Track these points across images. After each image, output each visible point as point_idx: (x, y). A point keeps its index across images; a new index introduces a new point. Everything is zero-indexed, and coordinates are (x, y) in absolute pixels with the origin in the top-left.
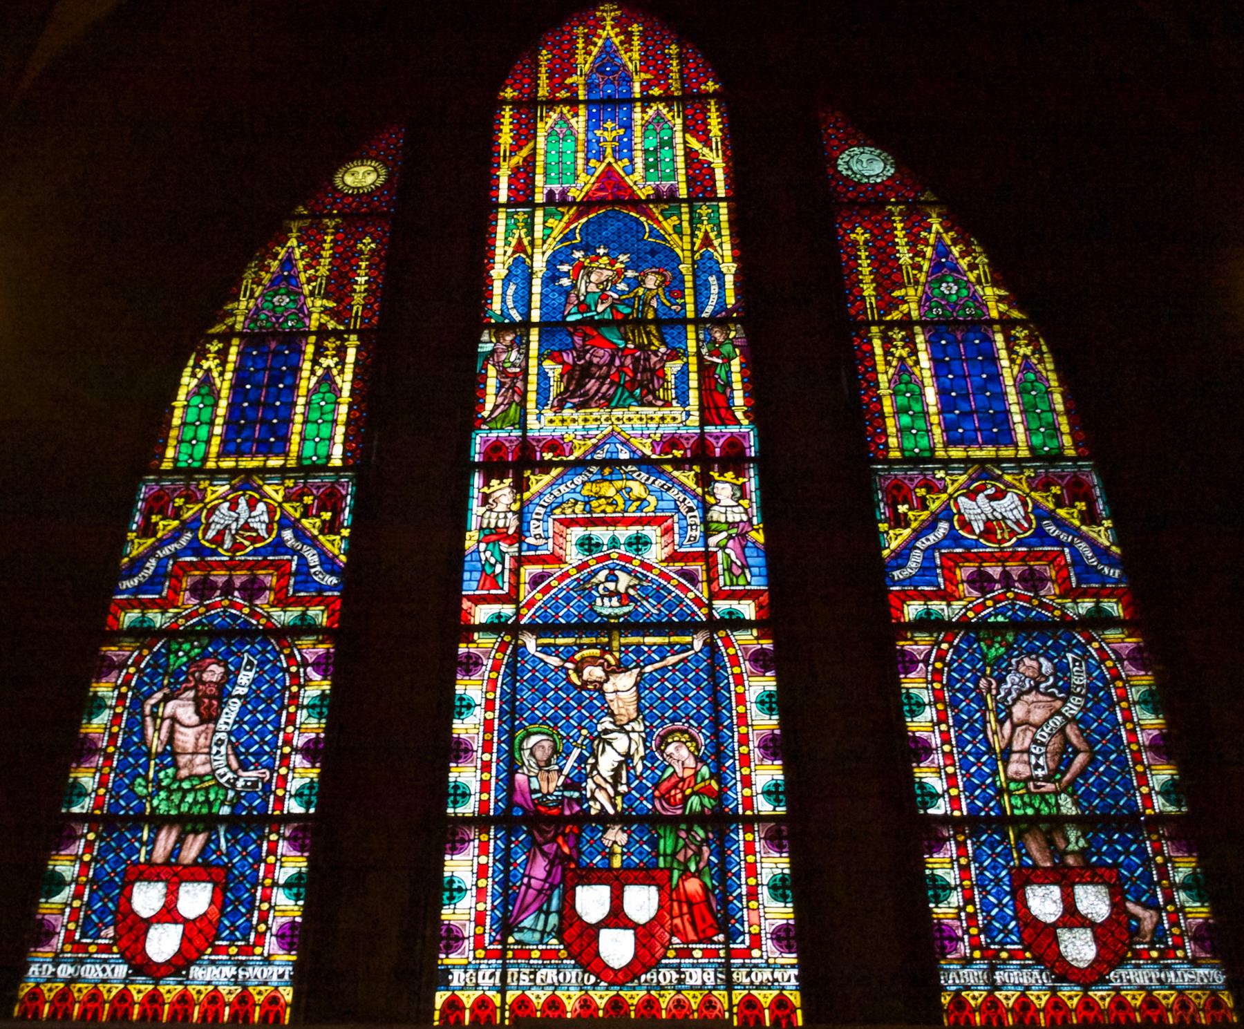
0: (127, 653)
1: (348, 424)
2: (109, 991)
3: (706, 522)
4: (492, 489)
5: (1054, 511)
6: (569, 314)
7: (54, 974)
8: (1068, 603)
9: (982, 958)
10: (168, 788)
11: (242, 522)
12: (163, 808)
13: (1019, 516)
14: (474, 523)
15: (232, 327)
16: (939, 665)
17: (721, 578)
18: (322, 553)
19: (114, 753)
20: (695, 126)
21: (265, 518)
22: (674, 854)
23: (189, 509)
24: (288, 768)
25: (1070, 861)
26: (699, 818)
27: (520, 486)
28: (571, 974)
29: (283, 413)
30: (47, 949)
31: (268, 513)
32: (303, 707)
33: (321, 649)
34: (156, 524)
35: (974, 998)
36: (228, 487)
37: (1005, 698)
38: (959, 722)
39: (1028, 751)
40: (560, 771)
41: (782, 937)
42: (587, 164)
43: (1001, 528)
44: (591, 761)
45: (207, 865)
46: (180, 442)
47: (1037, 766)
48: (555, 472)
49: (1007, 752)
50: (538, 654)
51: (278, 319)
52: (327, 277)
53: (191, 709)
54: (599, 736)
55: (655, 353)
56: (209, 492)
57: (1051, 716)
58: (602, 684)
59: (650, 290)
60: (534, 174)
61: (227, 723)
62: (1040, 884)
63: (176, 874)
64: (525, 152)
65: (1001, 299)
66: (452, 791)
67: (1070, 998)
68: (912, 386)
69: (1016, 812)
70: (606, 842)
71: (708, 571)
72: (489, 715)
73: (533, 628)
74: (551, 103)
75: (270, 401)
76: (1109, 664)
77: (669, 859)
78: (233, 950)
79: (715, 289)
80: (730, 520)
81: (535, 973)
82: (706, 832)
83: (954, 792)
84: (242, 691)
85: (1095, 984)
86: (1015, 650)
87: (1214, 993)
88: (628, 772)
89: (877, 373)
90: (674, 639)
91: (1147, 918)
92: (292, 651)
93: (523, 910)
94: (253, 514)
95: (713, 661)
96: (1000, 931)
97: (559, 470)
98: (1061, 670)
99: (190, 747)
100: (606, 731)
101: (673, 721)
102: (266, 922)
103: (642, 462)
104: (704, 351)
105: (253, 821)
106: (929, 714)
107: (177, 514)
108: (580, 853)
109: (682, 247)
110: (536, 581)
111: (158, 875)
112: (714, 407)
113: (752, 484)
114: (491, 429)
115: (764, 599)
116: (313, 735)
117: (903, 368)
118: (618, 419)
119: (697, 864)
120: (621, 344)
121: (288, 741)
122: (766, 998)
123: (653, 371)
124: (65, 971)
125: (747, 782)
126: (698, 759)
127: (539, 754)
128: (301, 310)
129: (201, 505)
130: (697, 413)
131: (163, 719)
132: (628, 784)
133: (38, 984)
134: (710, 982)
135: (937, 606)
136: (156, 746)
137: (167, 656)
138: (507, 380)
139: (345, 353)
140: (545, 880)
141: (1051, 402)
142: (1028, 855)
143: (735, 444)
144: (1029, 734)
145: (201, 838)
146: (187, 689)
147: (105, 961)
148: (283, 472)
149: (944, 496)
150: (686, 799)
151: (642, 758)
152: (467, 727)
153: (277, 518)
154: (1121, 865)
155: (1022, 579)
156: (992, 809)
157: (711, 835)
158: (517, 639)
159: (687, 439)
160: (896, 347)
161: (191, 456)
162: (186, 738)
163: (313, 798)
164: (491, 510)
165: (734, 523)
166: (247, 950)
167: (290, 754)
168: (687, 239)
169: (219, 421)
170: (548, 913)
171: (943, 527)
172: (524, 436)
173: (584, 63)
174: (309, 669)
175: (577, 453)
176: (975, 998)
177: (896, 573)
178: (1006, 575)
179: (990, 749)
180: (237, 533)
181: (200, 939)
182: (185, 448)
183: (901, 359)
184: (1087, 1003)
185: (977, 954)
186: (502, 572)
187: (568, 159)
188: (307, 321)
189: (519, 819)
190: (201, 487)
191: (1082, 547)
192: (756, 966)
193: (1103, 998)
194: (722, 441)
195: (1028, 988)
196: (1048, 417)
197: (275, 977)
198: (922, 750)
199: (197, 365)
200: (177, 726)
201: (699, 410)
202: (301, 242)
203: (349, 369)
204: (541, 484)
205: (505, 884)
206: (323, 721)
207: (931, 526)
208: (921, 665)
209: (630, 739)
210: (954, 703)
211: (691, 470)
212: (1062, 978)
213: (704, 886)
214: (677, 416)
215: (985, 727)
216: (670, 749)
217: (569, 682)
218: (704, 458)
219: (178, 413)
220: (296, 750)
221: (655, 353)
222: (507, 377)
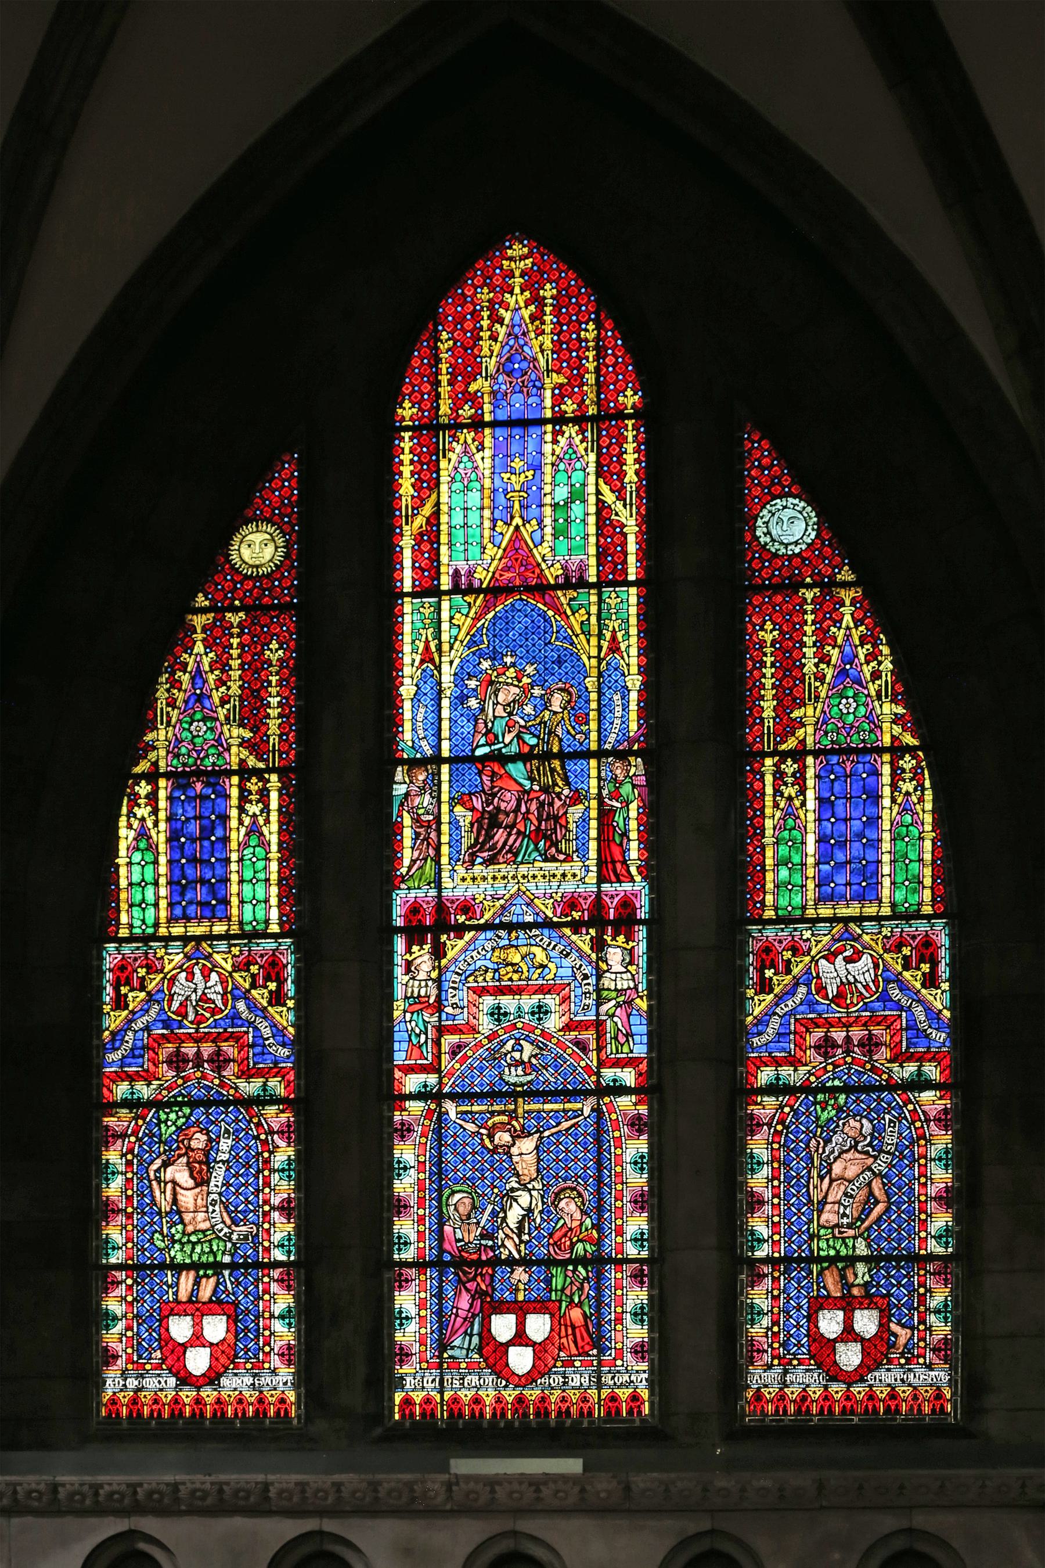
0: (126, 1124)
1: (279, 884)
2: (166, 1396)
3: (598, 990)
4: (414, 956)
5: (900, 974)
6: (478, 746)
7: (125, 1385)
8: (895, 1067)
9: (779, 1365)
10: (180, 1241)
11: (200, 993)
12: (179, 1258)
13: (869, 979)
14: (399, 992)
15: (155, 765)
16: (779, 1128)
17: (609, 1046)
18: (274, 1025)
19: (133, 1213)
20: (608, 469)
21: (219, 988)
22: (563, 1290)
23: (152, 980)
24: (269, 1223)
25: (855, 1291)
26: (583, 1261)
27: (438, 952)
28: (490, 1379)
29: (219, 871)
30: (115, 1368)
31: (222, 983)
32: (275, 1171)
33: (284, 1117)
34: (126, 996)
35: (769, 1393)
36: (181, 955)
37: (829, 1156)
38: (788, 1178)
39: (839, 1203)
40: (478, 1223)
41: (639, 1351)
42: (493, 529)
43: (852, 993)
44: (501, 1215)
45: (219, 1302)
46: (131, 906)
47: (844, 1215)
48: (468, 936)
49: (823, 1202)
50: (458, 1121)
51: (198, 752)
52: (240, 696)
53: (186, 1174)
54: (507, 1194)
55: (559, 795)
56: (166, 961)
57: (862, 1173)
58: (509, 1147)
59: (555, 713)
60: (439, 544)
61: (217, 1186)
62: (829, 1309)
63: (198, 1309)
64: (427, 510)
65: (897, 720)
66: (396, 1241)
67: (837, 1392)
68: (794, 832)
69: (822, 1253)
70: (512, 1281)
71: (598, 1039)
72: (422, 1176)
73: (453, 1096)
74: (456, 426)
75: (206, 857)
76: (918, 1124)
77: (559, 1293)
78: (249, 1366)
79: (618, 711)
80: (619, 987)
81: (463, 1379)
82: (587, 1272)
83: (776, 1237)
84: (225, 1157)
85: (856, 1382)
86: (844, 1111)
87: (939, 1388)
88: (529, 1224)
89: (763, 816)
90: (568, 1106)
91: (903, 1334)
92: (260, 1120)
93: (454, 1333)
94: (209, 984)
95: (598, 1126)
96: (795, 1345)
97: (473, 933)
98: (878, 1131)
99: (191, 1206)
100: (513, 1190)
101: (565, 1180)
102: (269, 1345)
103: (547, 924)
104: (605, 792)
105: (251, 1266)
106: (765, 1171)
107: (142, 988)
108: (494, 1289)
109: (588, 649)
110: (454, 1052)
111: (185, 1311)
112: (610, 867)
113: (642, 948)
114: (409, 889)
115: (643, 1067)
116: (286, 1196)
117: (789, 813)
118: (524, 877)
119: (580, 1297)
120: (527, 784)
121: (266, 1202)
122: (624, 1394)
123: (556, 818)
124: (132, 1383)
125: (620, 1232)
126: (584, 1213)
127: (461, 1209)
128: (218, 740)
129: (162, 975)
130: (595, 869)
131: (166, 1183)
132: (529, 1234)
133: (114, 1393)
134: (586, 1384)
135: (786, 1071)
136: (165, 1206)
137: (158, 1125)
138: (421, 830)
139: (268, 796)
140: (469, 1311)
141: (921, 851)
142: (824, 1287)
143: (627, 904)
144: (843, 1188)
145: (212, 1281)
146: (180, 1156)
147: (159, 1375)
148: (227, 937)
149: (807, 959)
150: (573, 1245)
151: (541, 1212)
152: (404, 1186)
153: (229, 989)
154: (892, 1295)
155: (861, 1044)
156: (803, 1251)
157: (590, 1274)
158: (441, 1107)
159: (585, 899)
160: (786, 784)
161: (143, 921)
162: (187, 1199)
163: (292, 1248)
164: (413, 978)
165: (622, 990)
166: (258, 1365)
167: (270, 1211)
168: (594, 641)
169: (163, 881)
170: (471, 1336)
171: (802, 990)
172: (439, 896)
173: (490, 354)
174: (276, 1137)
175: (487, 916)
176: (770, 1392)
177: (755, 1040)
178: (848, 1039)
179: (810, 1201)
180: (197, 1005)
181: (225, 1359)
182: (136, 912)
183: (790, 799)
184: (848, 1396)
185: (776, 1362)
186: (426, 1042)
187: (474, 518)
188: (227, 755)
189: (449, 1264)
190: (158, 956)
191: (919, 1011)
192: (618, 1372)
193: (859, 1393)
194: (616, 900)
195: (808, 1386)
196: (914, 867)
197: (281, 1384)
198: (756, 1202)
199: (131, 814)
200: (178, 1188)
201: (597, 865)
202: (208, 645)
203: (274, 817)
204: (457, 949)
205: (440, 1313)
206: (292, 1183)
207: (792, 992)
208: (765, 1127)
209: (531, 1196)
210: (787, 1164)
211: (588, 933)
212: (833, 1379)
213: (584, 1314)
214: (578, 872)
215: (808, 1182)
216: (562, 1204)
217: (484, 1146)
218: (601, 920)
219: (123, 871)
220: (273, 1208)
221: (559, 795)
222: (421, 827)
